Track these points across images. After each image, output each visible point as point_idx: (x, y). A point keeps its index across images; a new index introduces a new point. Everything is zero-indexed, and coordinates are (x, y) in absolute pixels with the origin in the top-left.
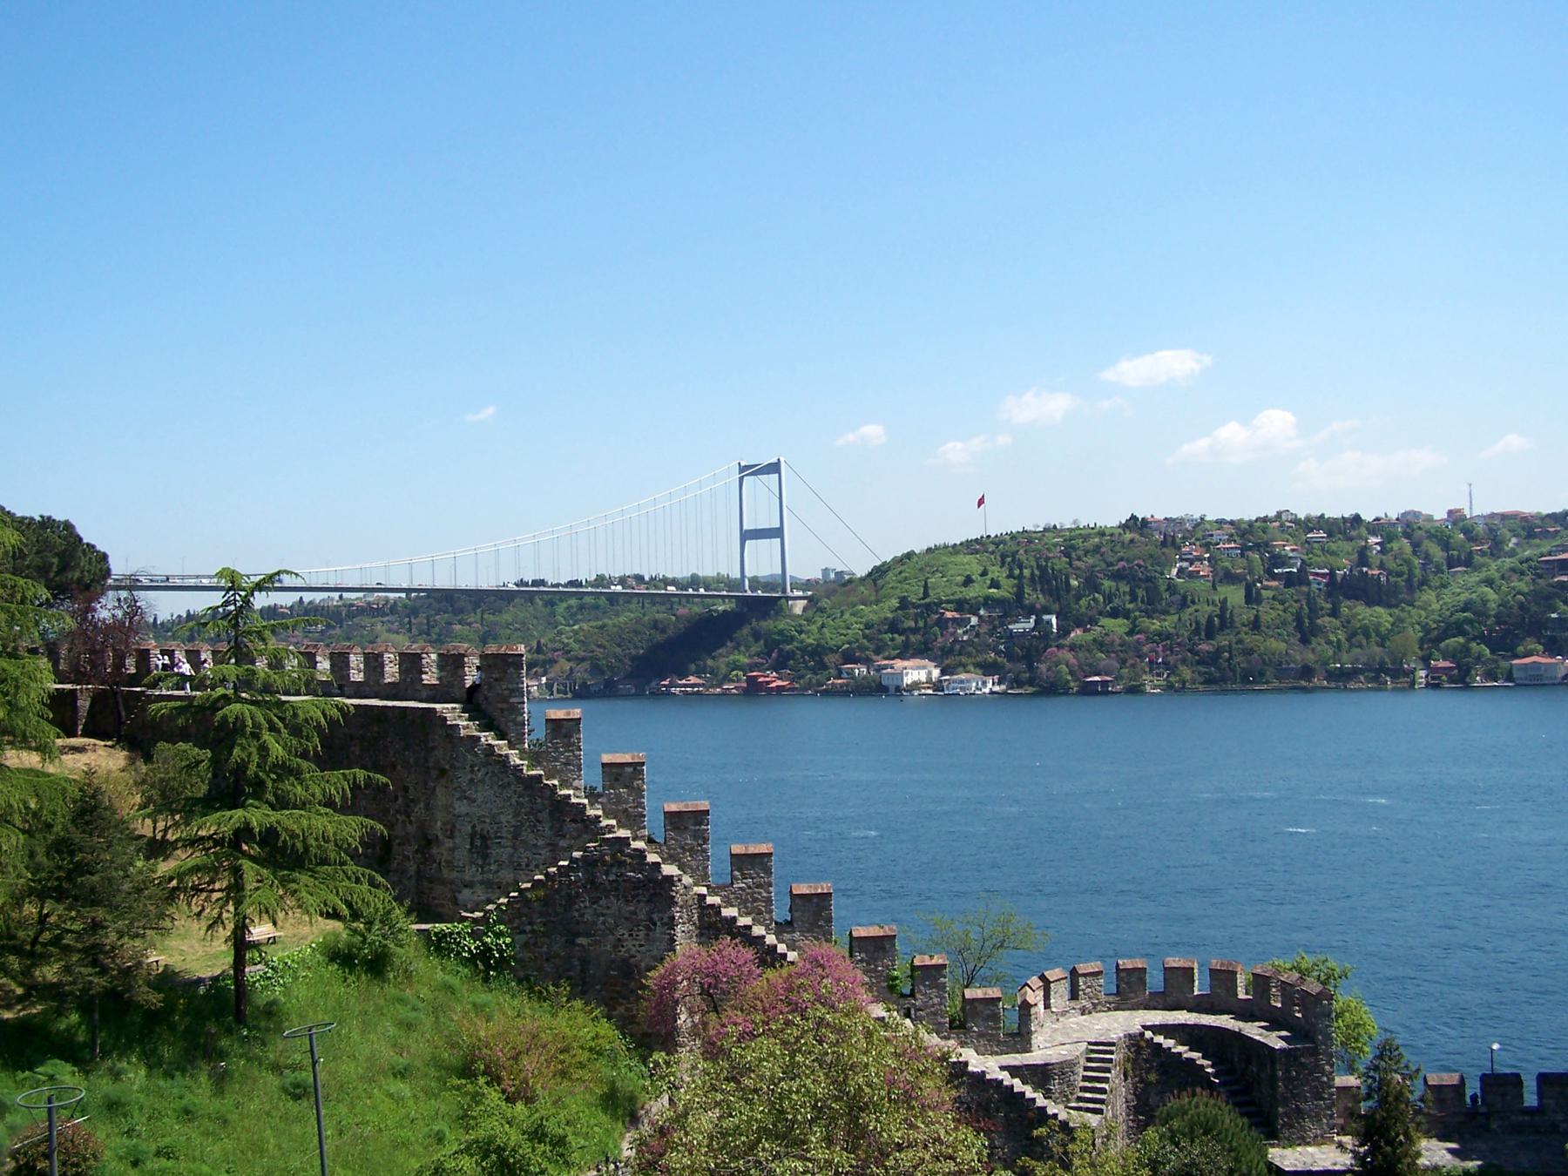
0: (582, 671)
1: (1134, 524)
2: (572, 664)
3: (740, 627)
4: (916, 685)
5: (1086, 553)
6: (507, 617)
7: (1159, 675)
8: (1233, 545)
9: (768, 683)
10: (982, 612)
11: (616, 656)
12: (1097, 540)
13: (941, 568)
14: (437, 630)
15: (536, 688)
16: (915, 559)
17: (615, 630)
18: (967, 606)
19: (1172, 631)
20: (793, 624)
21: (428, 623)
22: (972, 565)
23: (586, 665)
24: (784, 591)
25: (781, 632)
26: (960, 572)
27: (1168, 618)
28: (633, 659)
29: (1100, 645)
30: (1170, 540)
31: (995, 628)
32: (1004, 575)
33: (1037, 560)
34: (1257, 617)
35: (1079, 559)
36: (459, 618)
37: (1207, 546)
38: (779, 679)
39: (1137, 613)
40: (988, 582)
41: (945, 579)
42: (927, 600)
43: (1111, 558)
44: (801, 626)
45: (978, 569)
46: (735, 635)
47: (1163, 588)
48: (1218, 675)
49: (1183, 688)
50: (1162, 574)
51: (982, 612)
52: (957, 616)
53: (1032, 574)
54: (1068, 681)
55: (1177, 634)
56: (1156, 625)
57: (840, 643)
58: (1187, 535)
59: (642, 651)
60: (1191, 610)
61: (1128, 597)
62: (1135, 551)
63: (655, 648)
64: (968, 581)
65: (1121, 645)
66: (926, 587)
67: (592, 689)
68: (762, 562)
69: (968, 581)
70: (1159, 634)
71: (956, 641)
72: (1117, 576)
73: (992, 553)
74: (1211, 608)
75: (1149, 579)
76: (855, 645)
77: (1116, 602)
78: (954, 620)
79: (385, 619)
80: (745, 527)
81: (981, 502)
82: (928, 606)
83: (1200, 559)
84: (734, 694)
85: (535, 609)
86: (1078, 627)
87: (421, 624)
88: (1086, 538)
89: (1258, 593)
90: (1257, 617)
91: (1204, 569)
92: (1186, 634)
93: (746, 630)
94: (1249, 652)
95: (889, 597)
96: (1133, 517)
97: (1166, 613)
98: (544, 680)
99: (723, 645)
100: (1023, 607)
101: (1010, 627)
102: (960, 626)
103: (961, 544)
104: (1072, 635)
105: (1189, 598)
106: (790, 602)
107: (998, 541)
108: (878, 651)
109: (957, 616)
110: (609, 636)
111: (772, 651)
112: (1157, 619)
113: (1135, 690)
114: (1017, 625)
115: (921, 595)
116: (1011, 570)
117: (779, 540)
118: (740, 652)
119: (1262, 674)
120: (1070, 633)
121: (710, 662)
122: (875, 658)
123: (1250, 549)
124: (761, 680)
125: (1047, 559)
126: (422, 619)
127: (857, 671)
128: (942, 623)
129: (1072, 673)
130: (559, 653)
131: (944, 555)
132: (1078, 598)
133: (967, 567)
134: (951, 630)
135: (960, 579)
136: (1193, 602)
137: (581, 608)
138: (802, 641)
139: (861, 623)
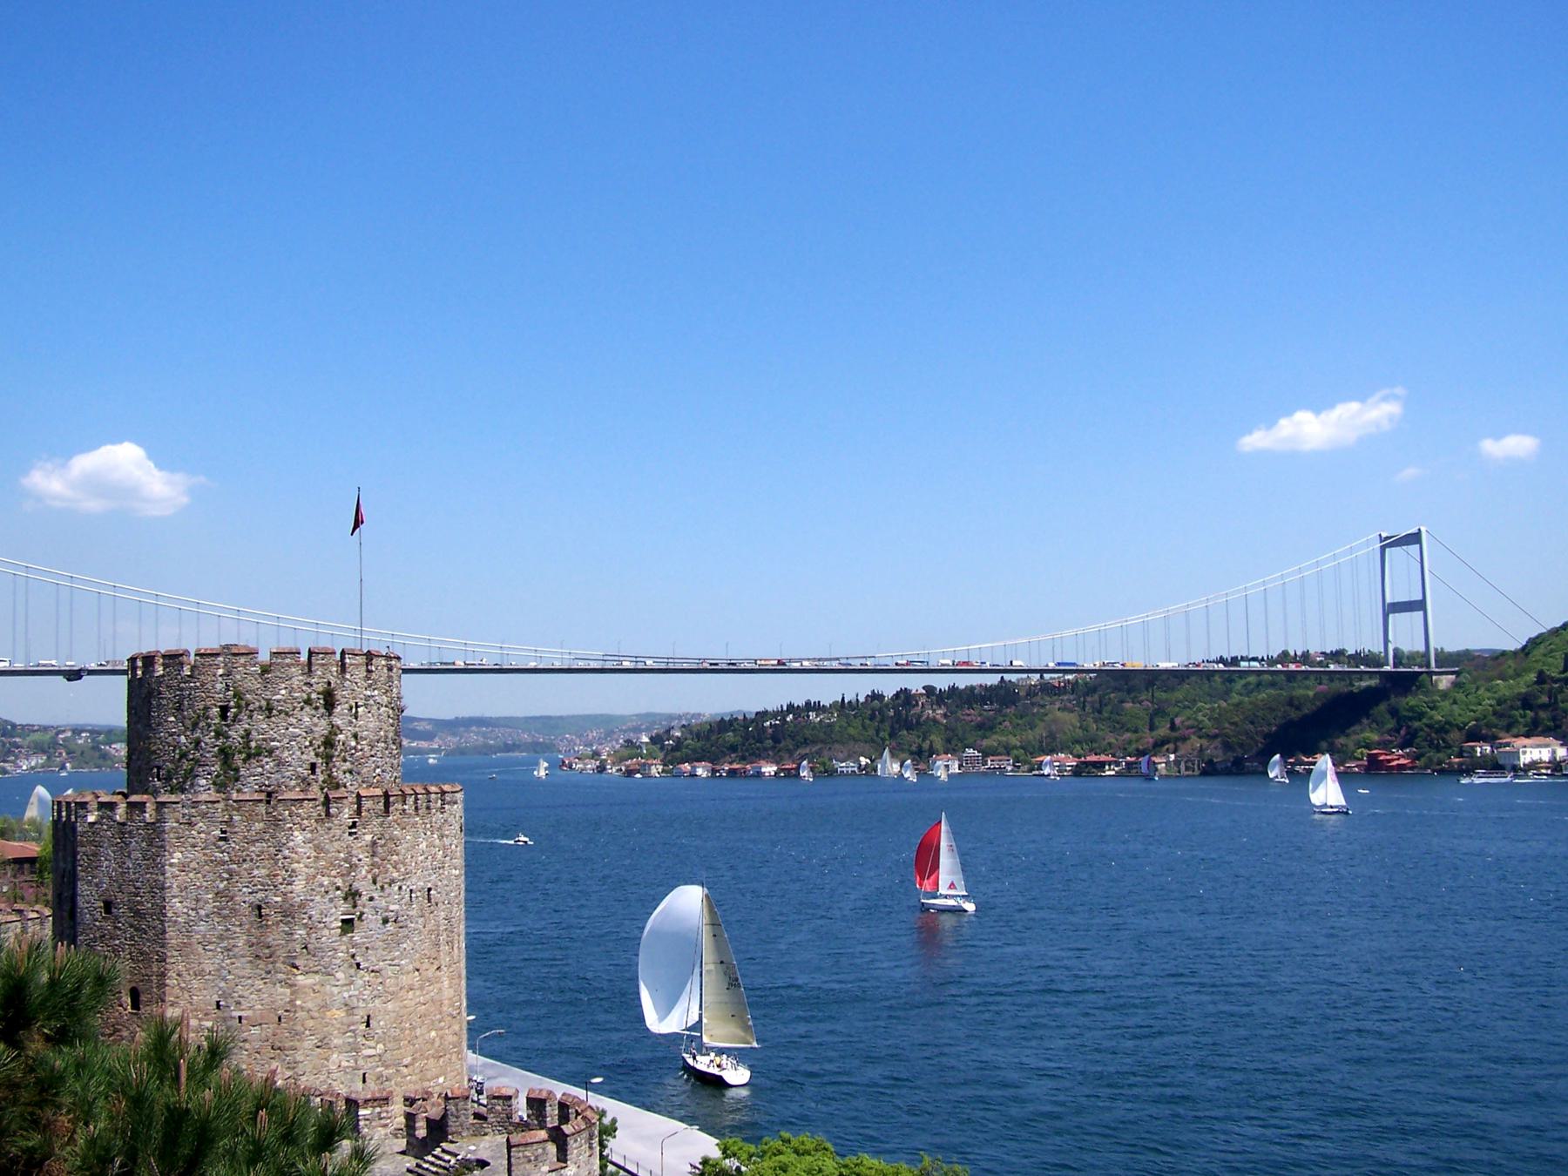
0: (1215, 752)
2: (1205, 742)
4: (1533, 765)
6: (1179, 695)
9: (1389, 761)
11: (1247, 733)
14: (1109, 708)
17: (1250, 707)
20: (1426, 699)
21: (1100, 701)
23: (1217, 742)
24: (1428, 665)
25: (1411, 709)
28: (1266, 736)
36: (1132, 695)
38: (1402, 756)
44: (1433, 702)
46: (1371, 712)
63: (1288, 726)
67: (1219, 767)
68: (1406, 635)
79: (1066, 698)
80: (1388, 600)
84: (1355, 773)
85: (1210, 687)
87: (1092, 702)
93: (1383, 707)
95: (1528, 670)
98: (1172, 757)
99: (1359, 722)
106: (1434, 678)
108: (1508, 728)
110: (1243, 713)
111: (1400, 729)
115: (1561, 669)
117: (1421, 613)
121: (1342, 740)
122: (1501, 735)
124: (1381, 758)
126: (1096, 697)
127: (1479, 750)
130: (1193, 730)
137: (1259, 684)
138: (1431, 718)
139: (1493, 698)
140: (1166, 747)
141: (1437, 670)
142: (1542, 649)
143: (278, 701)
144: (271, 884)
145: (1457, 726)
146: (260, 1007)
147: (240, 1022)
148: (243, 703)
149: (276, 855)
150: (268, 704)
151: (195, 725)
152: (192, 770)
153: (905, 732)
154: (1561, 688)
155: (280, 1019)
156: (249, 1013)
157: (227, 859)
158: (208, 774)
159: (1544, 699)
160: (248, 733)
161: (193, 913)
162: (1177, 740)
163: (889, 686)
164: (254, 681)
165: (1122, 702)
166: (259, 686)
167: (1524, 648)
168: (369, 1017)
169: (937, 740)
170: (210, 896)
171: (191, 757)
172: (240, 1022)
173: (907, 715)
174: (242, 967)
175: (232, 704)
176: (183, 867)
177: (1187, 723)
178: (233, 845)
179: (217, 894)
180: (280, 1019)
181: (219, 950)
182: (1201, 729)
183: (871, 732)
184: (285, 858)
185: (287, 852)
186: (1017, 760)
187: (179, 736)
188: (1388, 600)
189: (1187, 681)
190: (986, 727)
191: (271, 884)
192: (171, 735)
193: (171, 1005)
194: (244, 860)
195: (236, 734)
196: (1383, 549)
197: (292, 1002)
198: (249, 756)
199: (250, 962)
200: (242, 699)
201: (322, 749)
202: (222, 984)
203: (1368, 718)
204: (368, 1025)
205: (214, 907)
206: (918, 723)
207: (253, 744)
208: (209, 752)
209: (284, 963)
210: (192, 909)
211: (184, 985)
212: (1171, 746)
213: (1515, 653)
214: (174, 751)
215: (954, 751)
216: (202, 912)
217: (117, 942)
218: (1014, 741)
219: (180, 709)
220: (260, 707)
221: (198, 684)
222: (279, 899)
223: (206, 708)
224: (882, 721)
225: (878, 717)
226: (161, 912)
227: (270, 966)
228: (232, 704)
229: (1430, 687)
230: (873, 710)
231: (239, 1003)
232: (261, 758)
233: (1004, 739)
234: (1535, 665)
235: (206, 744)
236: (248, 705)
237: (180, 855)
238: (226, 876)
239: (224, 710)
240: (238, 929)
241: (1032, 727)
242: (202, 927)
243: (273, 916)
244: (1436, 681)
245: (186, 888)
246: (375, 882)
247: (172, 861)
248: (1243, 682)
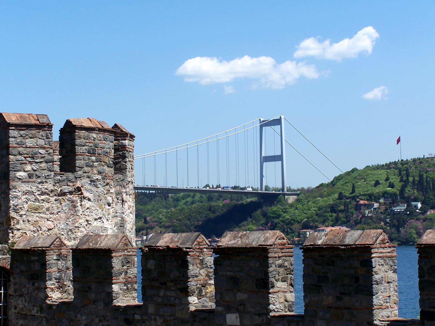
3: (256, 210)
6: (149, 207)
10: (382, 201)
11: (186, 225)
15: (140, 242)
16: (356, 172)
18: (373, 197)
22: (382, 175)
25: (274, 212)
32: (398, 180)
40: (388, 184)
41: (365, 183)
42: (353, 195)
45: (384, 177)
51: (382, 201)
52: (366, 202)
53: (414, 180)
57: (302, 218)
59: (200, 223)
63: (209, 220)
64: (377, 183)
66: (353, 187)
69: (377, 183)
71: (364, 216)
76: (310, 219)
78: (365, 205)
80: (263, 155)
81: (399, 141)
82: (354, 198)
85: (166, 203)
93: (259, 212)
95: (333, 193)
101: (393, 209)
102: (368, 208)
103: (386, 164)
104: (428, 213)
106: (286, 197)
107: (403, 163)
108: (323, 222)
109: (366, 202)
110: (184, 214)
114: (398, 208)
115: (351, 192)
116: (402, 178)
117: (280, 162)
118: (253, 224)
120: (427, 212)
122: (319, 226)
125: (427, 172)
127: (308, 233)
128: (358, 207)
130: (156, 223)
131: (370, 170)
133: (379, 176)
134: (362, 210)
135: (373, 183)
139: (316, 207)
140: (141, 232)
141: (287, 193)
142: (341, 182)
145: (297, 221)
154: (350, 202)
159: (342, 207)
162: (147, 228)
167: (332, 182)
177: (153, 220)
182: (161, 223)
188: (263, 155)
189: (154, 200)
196: (261, 127)
203: (251, 218)
212: (144, 232)
213: (328, 185)
229: (284, 202)
234: (338, 190)
244: (287, 199)
248: (184, 201)
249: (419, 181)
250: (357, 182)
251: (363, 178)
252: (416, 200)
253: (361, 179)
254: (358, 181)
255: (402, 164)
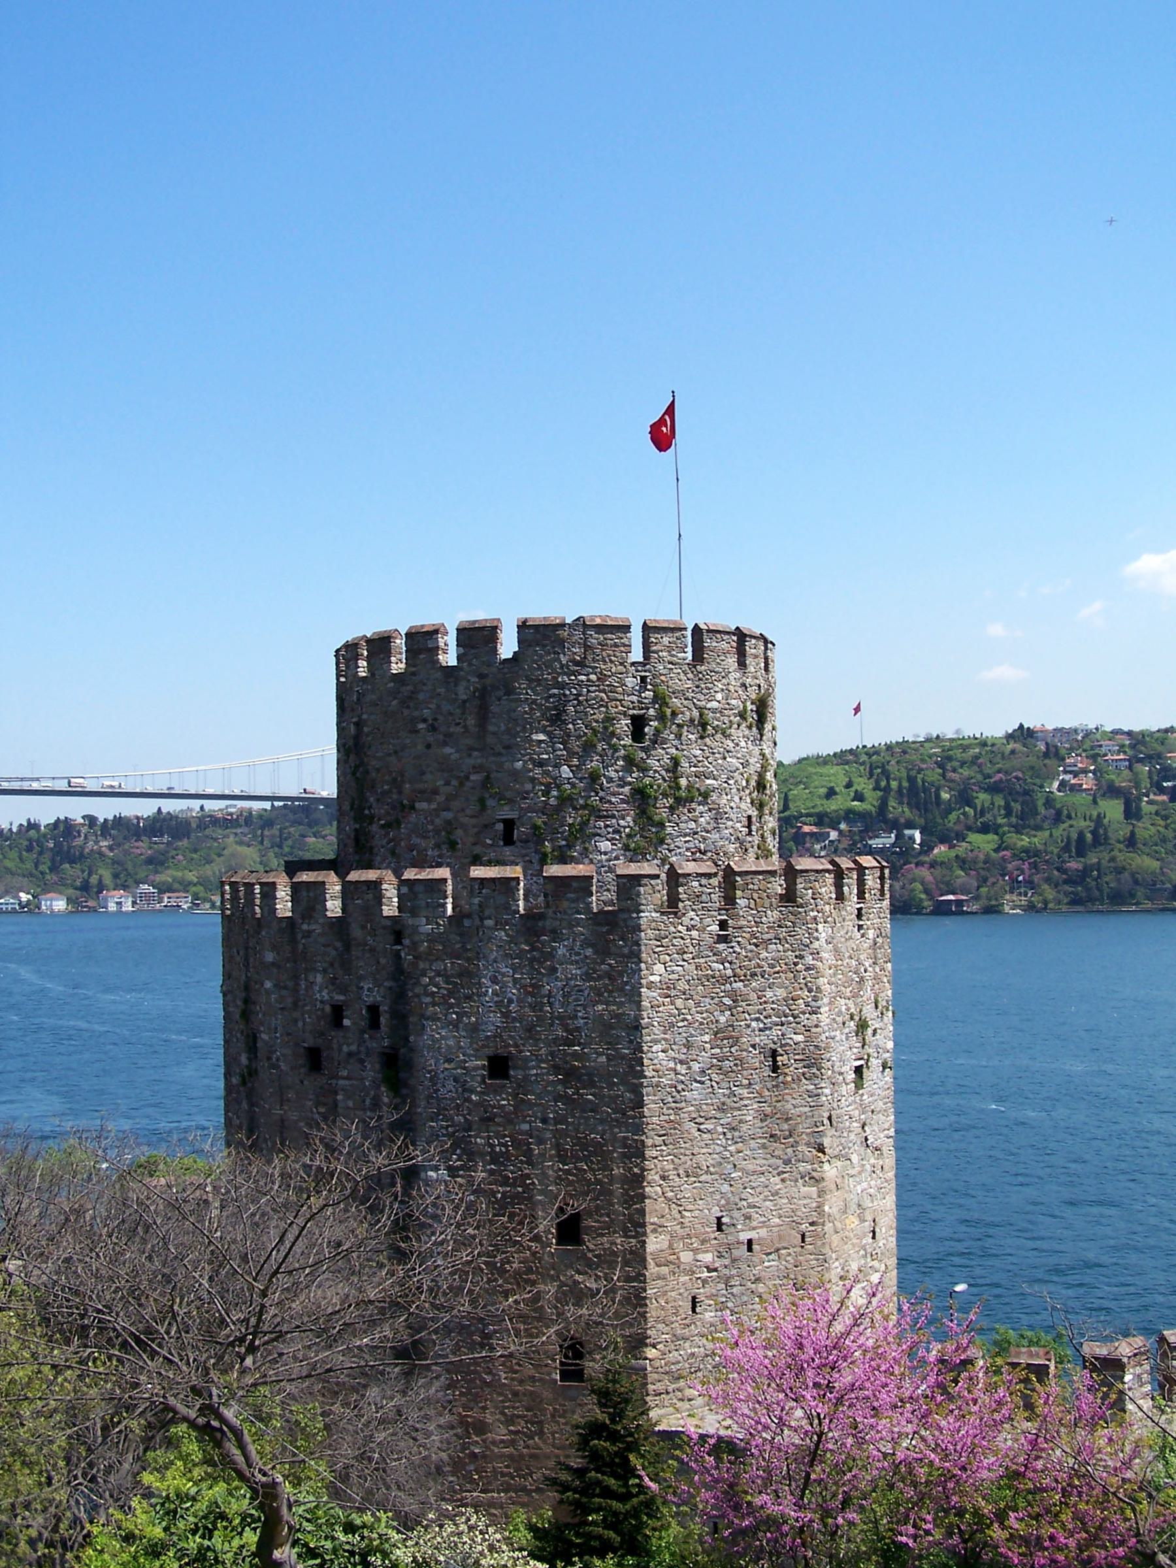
1: (1023, 734)
5: (963, 764)
7: (1020, 894)
8: (1122, 757)
10: (843, 826)
12: (977, 750)
13: (805, 780)
14: (290, 842)
18: (826, 820)
19: (1040, 847)
21: (280, 837)
22: (837, 776)
26: (825, 783)
27: (1039, 833)
29: (962, 862)
30: (1053, 750)
31: (855, 844)
32: (871, 787)
33: (909, 770)
34: (1133, 833)
35: (954, 771)
36: (314, 830)
37: (1094, 758)
39: (1006, 829)
40: (852, 794)
41: (807, 791)
43: (988, 769)
47: (1040, 803)
48: (1084, 895)
49: (1045, 908)
50: (1042, 787)
51: (843, 826)
53: (900, 786)
54: (921, 900)
55: (1045, 851)
56: (1025, 841)
58: (1075, 745)
60: (1065, 825)
61: (1003, 812)
62: (1016, 762)
64: (831, 793)
65: (985, 862)
69: (831, 793)
70: (1026, 851)
72: (994, 789)
73: (863, 763)
74: (1088, 823)
75: (1027, 793)
77: (988, 817)
78: (812, 834)
79: (239, 831)
81: (857, 710)
83: (1085, 771)
86: (942, 842)
87: (273, 836)
88: (965, 748)
89: (1139, 809)
90: (1133, 833)
91: (1088, 782)
92: (1056, 851)
94: (1120, 870)
96: (1021, 726)
97: (1038, 828)
100: (886, 821)
101: (870, 842)
102: (818, 841)
103: (835, 754)
104: (936, 851)
105: (1065, 812)
107: (873, 752)
112: (1027, 834)
113: (992, 910)
114: (877, 840)
116: (877, 782)
119: (1132, 895)
120: (933, 849)
123: (1140, 761)
125: (920, 771)
126: (275, 831)
129: (926, 891)
131: (811, 765)
132: (949, 811)
133: (832, 778)
134: (808, 845)
135: (823, 791)
136: (1069, 817)
143: (714, 711)
144: (788, 1014)
146: (777, 1220)
147: (750, 1249)
148: (668, 712)
149: (796, 964)
150: (701, 715)
151: (589, 747)
152: (585, 824)
153: (67, 866)
155: (803, 1236)
156: (763, 1232)
157: (729, 972)
158: (614, 832)
160: (676, 762)
161: (682, 1069)
163: (47, 812)
164: (682, 676)
165: (304, 836)
166: (689, 684)
168: (874, 1221)
169: (106, 875)
170: (707, 1038)
171: (581, 802)
172: (750, 1249)
173: (70, 847)
174: (753, 1157)
175: (652, 712)
176: (667, 989)
178: (738, 949)
179: (716, 1034)
180: (803, 1236)
181: (720, 1129)
183: (29, 865)
184: (808, 969)
185: (809, 960)
186: (196, 897)
187: (557, 766)
190: (157, 862)
191: (788, 1014)
192: (541, 764)
193: (654, 1231)
194: (754, 975)
195: (658, 761)
197: (820, 1206)
198: (679, 801)
199: (764, 1146)
200: (667, 704)
201: (756, 793)
202: (725, 1188)
204: (874, 1237)
205: (713, 1056)
206: (82, 856)
207: (683, 782)
208: (614, 794)
209: (808, 1144)
210: (681, 1062)
211: (670, 1194)
214: (546, 793)
215: (125, 887)
216: (696, 1067)
217: (525, 1127)
218: (191, 876)
219: (557, 718)
220: (692, 720)
221: (593, 677)
222: (800, 1038)
223: (609, 719)
224: (40, 853)
225: (37, 849)
226: (633, 1067)
227: (790, 1150)
228: (652, 712)
230: (30, 840)
231: (748, 1217)
232: (694, 805)
233: (180, 874)
235: (610, 780)
236: (674, 714)
237: (659, 968)
238: (728, 1001)
239: (638, 723)
240: (744, 1092)
241: (209, 862)
242: (695, 1093)
243: (792, 1066)
245: (672, 1025)
246: (877, 1007)
247: (652, 978)
249: (910, 789)
250: (791, 790)
251: (800, 782)
252: (910, 825)
253: (797, 784)
254: (792, 787)
255: (869, 755)
